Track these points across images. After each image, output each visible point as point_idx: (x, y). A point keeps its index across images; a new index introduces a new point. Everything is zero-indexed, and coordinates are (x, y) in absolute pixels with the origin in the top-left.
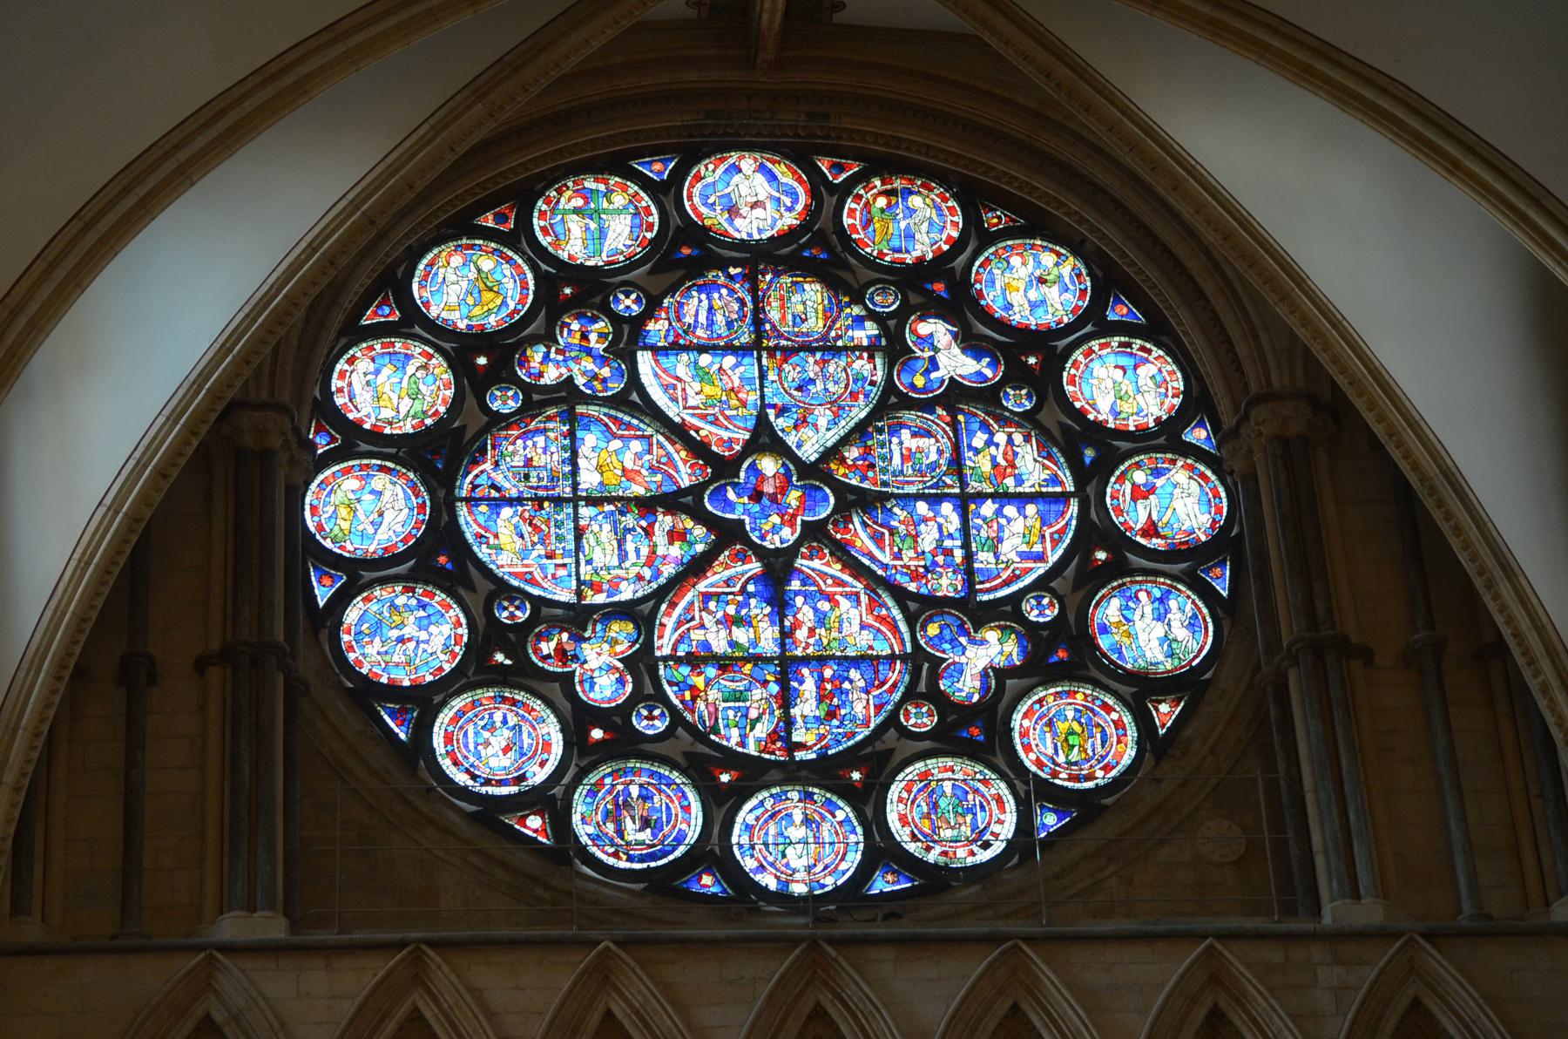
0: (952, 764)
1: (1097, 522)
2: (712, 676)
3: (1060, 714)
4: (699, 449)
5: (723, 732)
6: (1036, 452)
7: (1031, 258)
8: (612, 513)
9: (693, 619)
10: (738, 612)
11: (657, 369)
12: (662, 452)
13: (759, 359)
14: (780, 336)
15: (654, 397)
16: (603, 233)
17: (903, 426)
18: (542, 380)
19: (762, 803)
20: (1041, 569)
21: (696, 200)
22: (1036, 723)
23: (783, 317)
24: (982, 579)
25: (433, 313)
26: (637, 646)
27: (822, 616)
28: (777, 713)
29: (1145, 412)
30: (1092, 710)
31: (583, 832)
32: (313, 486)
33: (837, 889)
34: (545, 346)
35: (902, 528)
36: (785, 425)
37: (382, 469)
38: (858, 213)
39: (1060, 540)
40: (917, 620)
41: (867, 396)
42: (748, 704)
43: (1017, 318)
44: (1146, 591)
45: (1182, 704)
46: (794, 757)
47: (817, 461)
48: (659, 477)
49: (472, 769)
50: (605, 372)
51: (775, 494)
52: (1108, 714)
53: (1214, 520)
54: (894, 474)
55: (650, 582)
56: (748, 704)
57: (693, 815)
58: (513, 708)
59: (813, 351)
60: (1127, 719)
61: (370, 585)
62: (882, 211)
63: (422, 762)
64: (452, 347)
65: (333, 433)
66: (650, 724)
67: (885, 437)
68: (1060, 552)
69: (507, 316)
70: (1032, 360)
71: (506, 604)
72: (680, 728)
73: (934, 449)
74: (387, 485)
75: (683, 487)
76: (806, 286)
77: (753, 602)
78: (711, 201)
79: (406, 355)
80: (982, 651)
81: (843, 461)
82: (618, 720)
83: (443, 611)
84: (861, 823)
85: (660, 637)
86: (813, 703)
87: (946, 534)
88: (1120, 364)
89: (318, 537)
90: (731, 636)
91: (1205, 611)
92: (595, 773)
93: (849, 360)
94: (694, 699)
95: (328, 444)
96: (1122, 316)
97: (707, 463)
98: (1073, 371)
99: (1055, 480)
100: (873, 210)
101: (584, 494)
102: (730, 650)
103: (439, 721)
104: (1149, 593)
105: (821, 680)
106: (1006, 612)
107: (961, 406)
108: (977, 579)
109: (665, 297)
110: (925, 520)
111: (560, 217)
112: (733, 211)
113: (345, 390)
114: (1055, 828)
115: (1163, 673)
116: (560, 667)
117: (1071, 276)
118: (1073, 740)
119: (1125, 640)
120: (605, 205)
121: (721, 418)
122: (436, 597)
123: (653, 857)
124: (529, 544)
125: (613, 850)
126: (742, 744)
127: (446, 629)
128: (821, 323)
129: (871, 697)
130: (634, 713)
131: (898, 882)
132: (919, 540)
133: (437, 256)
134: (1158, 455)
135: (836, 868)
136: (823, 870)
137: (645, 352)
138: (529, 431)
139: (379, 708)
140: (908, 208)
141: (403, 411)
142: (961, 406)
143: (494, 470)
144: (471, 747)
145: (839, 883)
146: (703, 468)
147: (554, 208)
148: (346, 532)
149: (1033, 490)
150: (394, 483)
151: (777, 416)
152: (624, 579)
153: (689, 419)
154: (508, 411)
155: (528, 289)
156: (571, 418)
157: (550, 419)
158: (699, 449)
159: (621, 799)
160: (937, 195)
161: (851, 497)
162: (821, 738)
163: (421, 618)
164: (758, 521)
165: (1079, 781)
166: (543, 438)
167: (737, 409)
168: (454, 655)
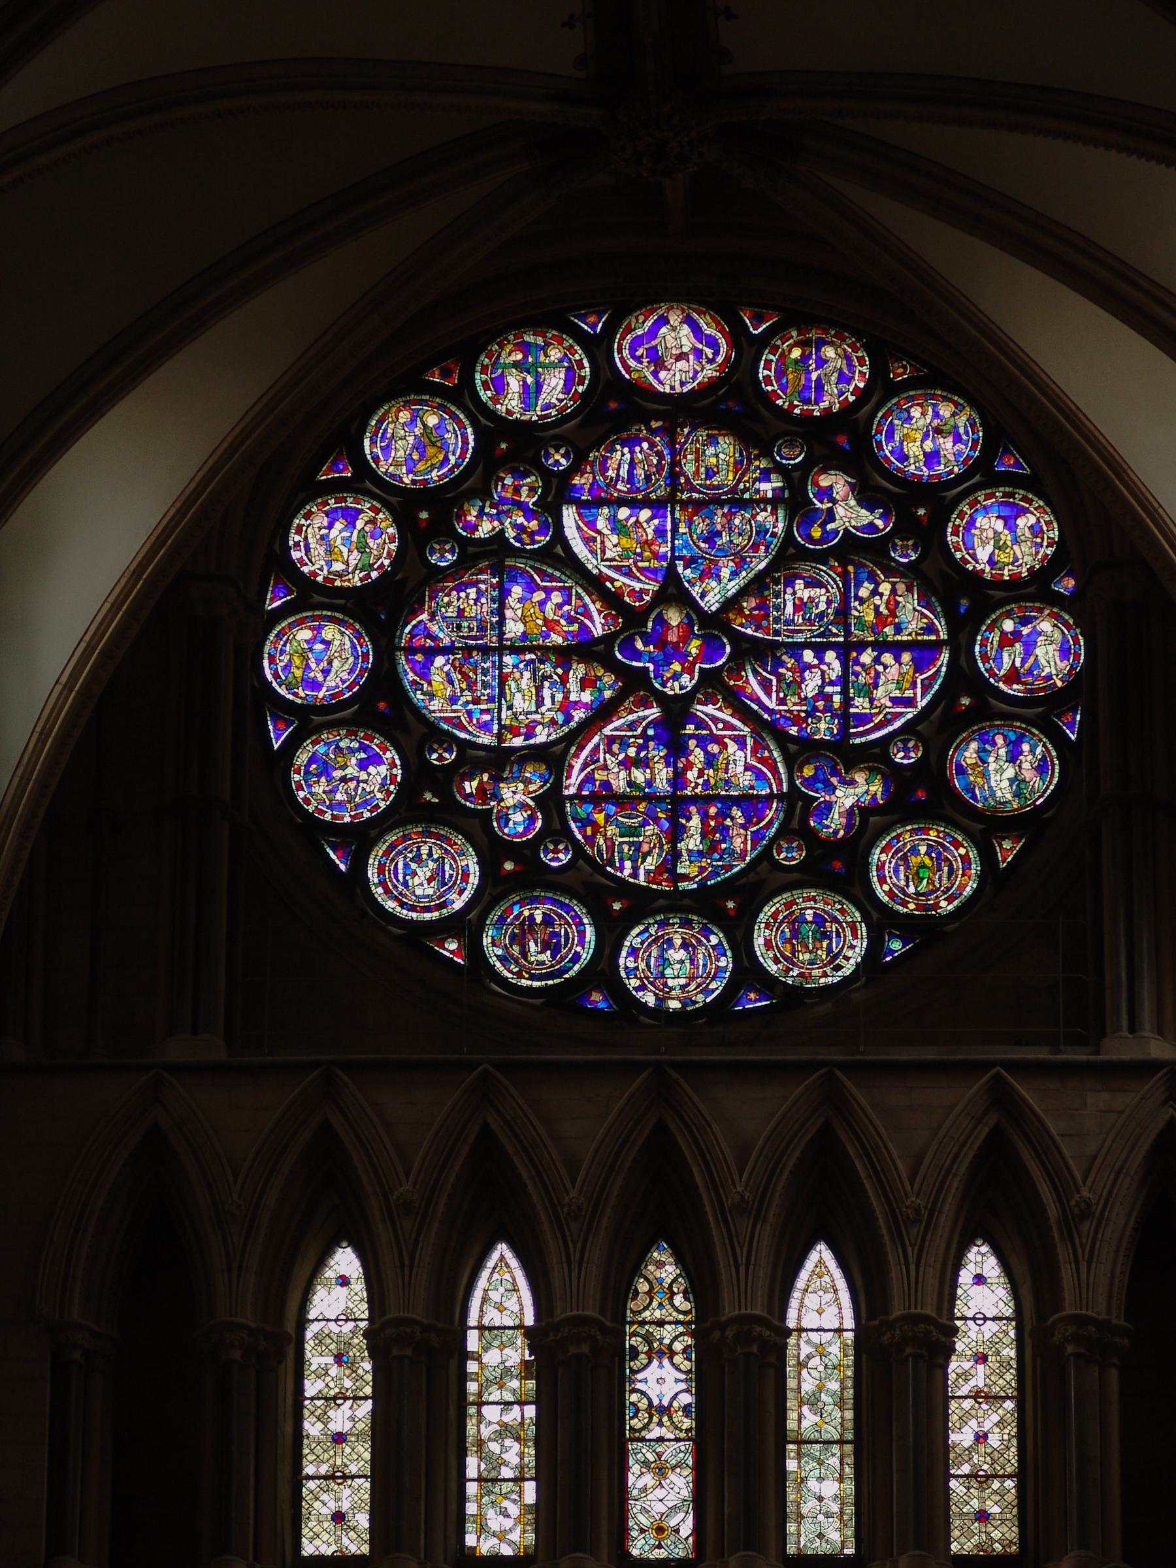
1: (966, 668)
3: (914, 851)
4: (612, 600)
5: (618, 865)
6: (916, 602)
7: (930, 409)
8: (532, 661)
9: (598, 761)
10: (638, 753)
11: (580, 522)
12: (579, 603)
14: (693, 489)
15: (576, 550)
18: (477, 533)
19: (646, 930)
23: (698, 469)
29: (1020, 561)
31: (493, 954)
32: (272, 637)
36: (691, 575)
37: (332, 620)
39: (931, 686)
42: (641, 839)
44: (1002, 734)
45: (1023, 841)
47: (718, 610)
48: (575, 627)
50: (534, 525)
51: (678, 643)
52: (957, 850)
53: (1072, 665)
55: (562, 726)
56: (641, 839)
57: (587, 940)
59: (722, 504)
61: (318, 729)
62: (796, 361)
63: (358, 891)
64: (398, 502)
67: (781, 587)
68: (929, 697)
71: (436, 746)
72: (581, 861)
73: (824, 598)
74: (336, 636)
76: (720, 439)
78: (638, 353)
82: (527, 852)
85: (569, 777)
87: (827, 680)
88: (1002, 514)
89: (274, 684)
91: (1054, 754)
93: (754, 512)
95: (285, 597)
97: (619, 614)
98: (958, 522)
99: (930, 629)
100: (788, 361)
102: (628, 790)
104: (1005, 738)
105: (705, 817)
108: (852, 723)
110: (810, 667)
111: (500, 371)
112: (658, 362)
113: (302, 544)
116: (480, 804)
117: (965, 427)
118: (924, 873)
119: (979, 780)
120: (542, 358)
121: (634, 570)
124: (458, 690)
125: (517, 969)
126: (635, 875)
128: (731, 478)
132: (803, 686)
133: (387, 412)
136: (695, 989)
141: (353, 563)
143: (431, 620)
144: (401, 880)
145: (708, 1000)
146: (615, 618)
147: (495, 362)
148: (299, 680)
149: (910, 638)
150: (342, 633)
151: (685, 568)
152: (540, 723)
153: (605, 570)
154: (445, 564)
155: (468, 444)
156: (497, 570)
157: (481, 572)
158: (612, 600)
160: (848, 345)
161: (745, 646)
162: (702, 870)
163: (361, 759)
166: (474, 590)
167: (649, 561)
168: (389, 793)
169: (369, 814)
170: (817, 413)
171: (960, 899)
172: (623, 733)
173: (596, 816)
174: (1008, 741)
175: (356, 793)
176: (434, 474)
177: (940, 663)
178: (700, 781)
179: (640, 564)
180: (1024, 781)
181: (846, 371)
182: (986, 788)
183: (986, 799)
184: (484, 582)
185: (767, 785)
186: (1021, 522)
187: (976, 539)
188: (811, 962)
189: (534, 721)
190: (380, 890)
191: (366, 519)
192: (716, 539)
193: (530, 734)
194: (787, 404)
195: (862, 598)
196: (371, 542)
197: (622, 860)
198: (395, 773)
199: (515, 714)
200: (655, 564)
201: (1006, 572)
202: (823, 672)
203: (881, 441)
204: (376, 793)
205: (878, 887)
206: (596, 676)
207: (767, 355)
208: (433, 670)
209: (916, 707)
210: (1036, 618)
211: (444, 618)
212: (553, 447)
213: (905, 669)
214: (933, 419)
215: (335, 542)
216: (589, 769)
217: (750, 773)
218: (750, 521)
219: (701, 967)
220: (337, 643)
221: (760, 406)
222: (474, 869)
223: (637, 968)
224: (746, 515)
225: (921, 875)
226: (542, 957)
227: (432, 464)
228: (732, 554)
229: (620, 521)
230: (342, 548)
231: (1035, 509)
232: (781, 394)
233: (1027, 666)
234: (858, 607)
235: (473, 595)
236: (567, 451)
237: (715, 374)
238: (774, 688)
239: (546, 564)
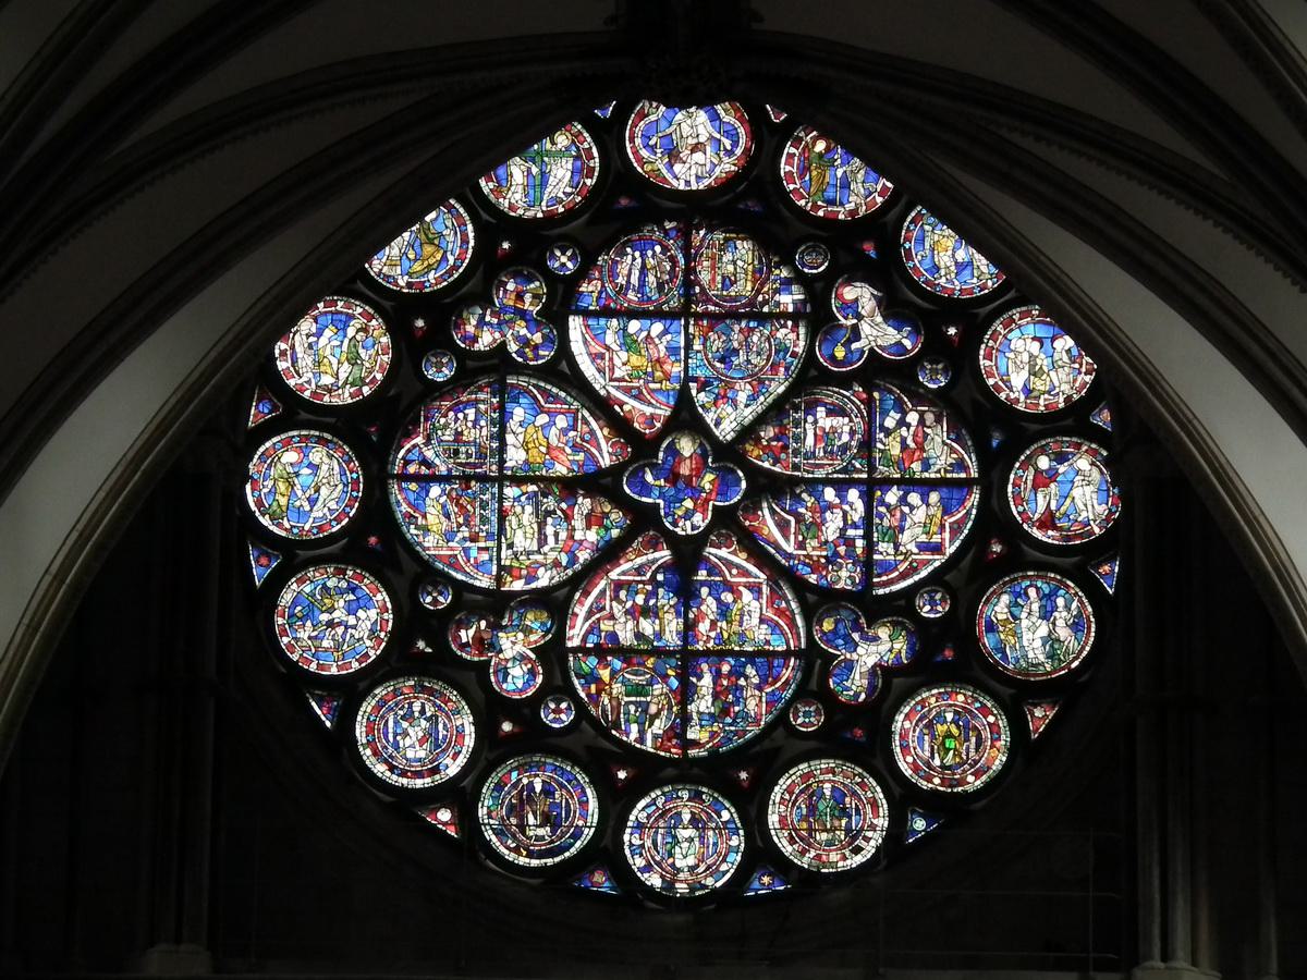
3: (940, 718)
4: (620, 426)
5: (623, 727)
6: (945, 434)
8: (535, 493)
9: (603, 608)
10: (646, 601)
12: (586, 429)
14: (708, 300)
15: (583, 367)
16: (544, 176)
17: (818, 403)
18: (476, 345)
20: (938, 561)
21: (638, 141)
22: (917, 725)
23: (714, 279)
24: (879, 571)
26: (550, 636)
27: (724, 608)
29: (1057, 390)
36: (706, 399)
37: (321, 441)
41: (787, 369)
42: (649, 699)
47: (733, 440)
48: (581, 457)
50: (537, 338)
51: (691, 476)
55: (566, 568)
56: (649, 699)
57: (590, 812)
59: (738, 317)
61: (305, 565)
62: (820, 155)
63: (345, 751)
66: (558, 716)
67: (801, 414)
68: (957, 543)
72: (584, 722)
73: (846, 429)
78: (652, 142)
79: (347, 314)
80: (873, 648)
81: (758, 440)
82: (526, 711)
85: (572, 627)
86: (709, 699)
87: (850, 522)
88: (1038, 335)
89: (257, 514)
90: (638, 628)
92: (504, 766)
97: (629, 442)
99: (960, 465)
101: (509, 473)
104: (1038, 589)
105: (717, 675)
106: (898, 609)
107: (877, 381)
110: (830, 507)
112: (673, 155)
113: (288, 353)
115: (1042, 675)
118: (950, 743)
119: (1011, 638)
120: (549, 146)
122: (365, 580)
124: (455, 525)
127: (373, 613)
128: (749, 288)
132: (824, 528)
134: (1065, 439)
136: (705, 871)
137: (577, 318)
138: (462, 402)
139: (308, 695)
141: (343, 376)
142: (877, 381)
143: (426, 444)
145: (718, 885)
148: (284, 509)
149: (938, 476)
150: (331, 457)
153: (614, 392)
155: (468, 243)
156: (501, 390)
157: (481, 389)
158: (620, 426)
162: (713, 735)
164: (672, 505)
166: (474, 410)
167: (661, 382)
169: (357, 664)
170: (841, 217)
171: (988, 774)
172: (631, 578)
174: (1041, 595)
175: (344, 640)
176: (432, 275)
178: (713, 634)
179: (652, 386)
180: (1058, 640)
183: (1017, 660)
188: (830, 843)
189: (536, 562)
190: (368, 752)
192: (733, 359)
193: (531, 578)
194: (810, 204)
195: (888, 428)
197: (627, 721)
198: (386, 618)
199: (515, 554)
200: (666, 385)
202: (845, 514)
203: (910, 248)
204: (367, 641)
205: (902, 759)
206: (603, 512)
207: (789, 149)
208: (428, 501)
209: (944, 554)
213: (932, 511)
215: (324, 352)
216: (593, 619)
217: (766, 626)
218: (768, 339)
220: (325, 467)
221: (781, 206)
222: (470, 729)
223: (642, 846)
224: (766, 331)
225: (947, 746)
226: (541, 832)
227: (429, 265)
228: (751, 376)
230: (331, 358)
233: (1063, 509)
235: (471, 417)
236: (574, 254)
237: (733, 168)
238: (793, 530)
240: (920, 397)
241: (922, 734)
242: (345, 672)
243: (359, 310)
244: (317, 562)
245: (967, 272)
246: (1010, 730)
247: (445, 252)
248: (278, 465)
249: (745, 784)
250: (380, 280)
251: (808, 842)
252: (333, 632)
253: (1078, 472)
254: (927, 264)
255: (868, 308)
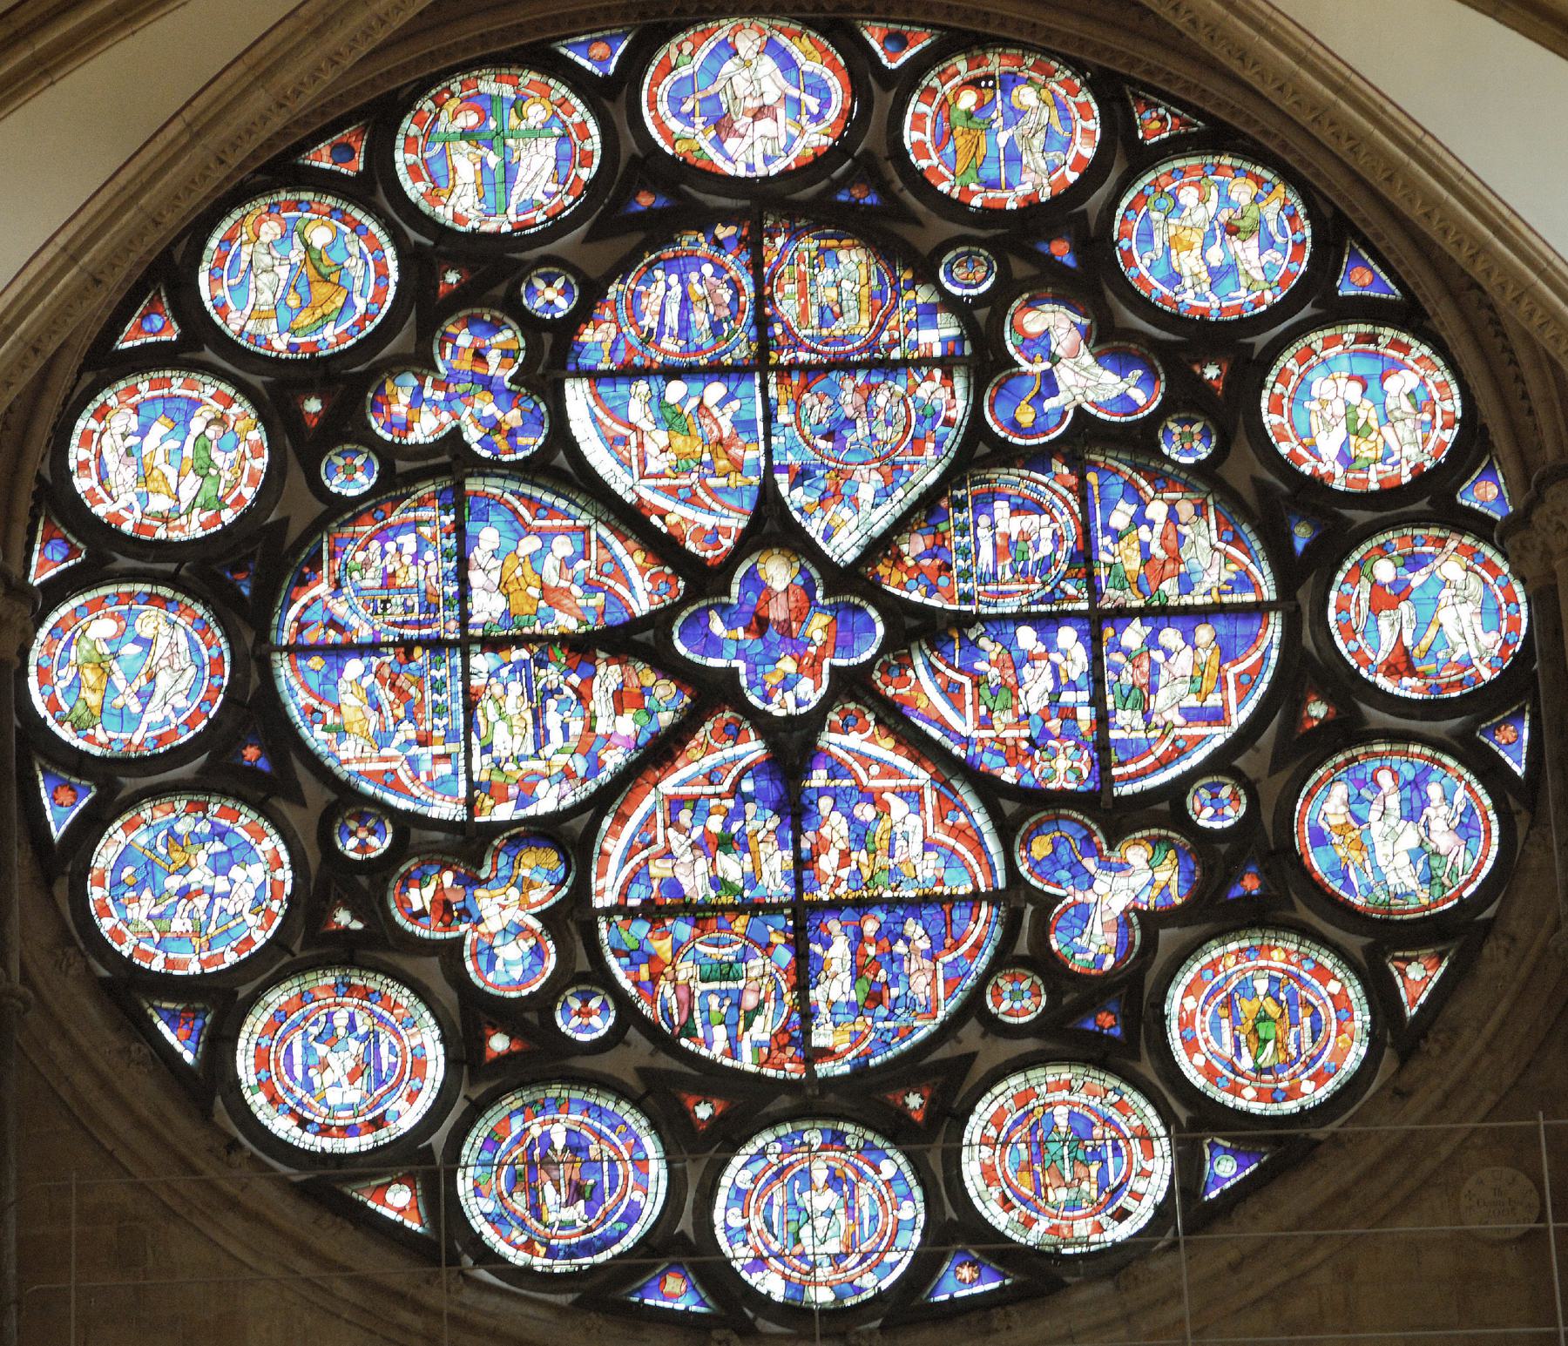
0: (1069, 1076)
1: (1314, 651)
2: (685, 939)
3: (1245, 987)
5: (700, 1033)
6: (1214, 534)
8: (525, 663)
10: (726, 826)
11: (597, 411)
12: (604, 555)
13: (764, 388)
14: (798, 345)
16: (509, 172)
17: (994, 495)
20: (1219, 736)
21: (663, 108)
22: (1206, 1002)
23: (804, 312)
24: (1122, 758)
25: (233, 326)
26: (565, 890)
28: (788, 998)
29: (1397, 456)
30: (1298, 978)
31: (477, 1209)
32: (42, 634)
33: (880, 1296)
34: (416, 375)
35: (993, 673)
36: (805, 499)
37: (151, 599)
38: (929, 121)
39: (1253, 684)
40: (1015, 830)
41: (939, 445)
43: (1189, 297)
44: (1390, 768)
45: (1445, 964)
46: (814, 1072)
47: (858, 561)
49: (299, 1110)
50: (514, 417)
51: (788, 622)
52: (1324, 983)
53: (1505, 642)
54: (982, 580)
55: (584, 780)
56: (741, 984)
57: (652, 1176)
58: (365, 1003)
59: (850, 368)
60: (1355, 991)
61: (134, 801)
62: (969, 115)
63: (218, 1099)
65: (74, 541)
67: (966, 515)
68: (1251, 706)
69: (354, 325)
70: (1211, 372)
71: (353, 825)
73: (1047, 534)
74: (161, 628)
75: (638, 614)
76: (842, 255)
77: (750, 808)
78: (687, 108)
80: (1120, 881)
81: (899, 557)
82: (532, 1017)
83: (253, 842)
84: (921, 1183)
85: (601, 874)
86: (846, 978)
87: (1064, 681)
88: (1358, 372)
89: (51, 722)
91: (1487, 801)
92: (496, 1108)
94: (654, 979)
95: (65, 560)
96: (1364, 287)
97: (678, 572)
99: (1244, 581)
100: (954, 115)
101: (479, 632)
102: (712, 894)
103: (246, 1029)
104: (1395, 774)
107: (1093, 457)
108: (1114, 759)
109: (610, 283)
110: (1030, 658)
111: (438, 147)
112: (722, 125)
113: (92, 464)
114: (1233, 1181)
115: (1415, 911)
118: (1264, 1030)
119: (1354, 854)
120: (514, 121)
121: (700, 492)
122: (242, 818)
123: (588, 1248)
124: (391, 721)
125: (524, 1238)
127: (257, 872)
128: (865, 321)
129: (939, 966)
130: (559, 1006)
131: (979, 1280)
132: (1021, 693)
133: (239, 223)
134: (1417, 532)
135: (880, 1259)
136: (860, 1263)
138: (390, 526)
139: (150, 1011)
140: (1012, 108)
142: (1093, 457)
145: (884, 1285)
147: (429, 132)
148: (96, 712)
149: (1208, 600)
150: (173, 624)
151: (793, 486)
153: (647, 495)
155: (387, 277)
157: (422, 503)
159: (537, 1151)
160: (1058, 83)
161: (911, 623)
162: (857, 1038)
163: (216, 854)
164: (760, 669)
165: (1275, 1101)
167: (726, 475)
168: (270, 916)
169: (234, 955)
170: (1011, 205)
172: (697, 790)
173: (657, 944)
175: (210, 918)
177: (1266, 643)
178: (844, 873)
179: (712, 482)
180: (1436, 854)
181: (1057, 127)
182: (1369, 869)
183: (1370, 890)
184: (428, 522)
185: (966, 876)
186: (1394, 384)
187: (1313, 419)
188: (1073, 1206)
189: (533, 773)
191: (209, 416)
192: (846, 433)
194: (957, 189)
196: (218, 457)
197: (707, 1023)
201: (1373, 476)
202: (1055, 669)
207: (916, 106)
208: (342, 686)
210: (1434, 556)
211: (358, 591)
212: (541, 276)
214: (1219, 209)
216: (637, 859)
218: (904, 399)
219: (866, 1222)
220: (162, 642)
222: (435, 1054)
223: (748, 1228)
225: (1262, 1035)
226: (568, 1214)
229: (670, 406)
230: (168, 470)
231: (1416, 361)
232: (947, 173)
233: (1424, 643)
234: (1111, 547)
238: (969, 698)
239: (540, 486)
240: (1163, 475)
241: (1217, 1017)
242: (214, 969)
243: (210, 391)
244: (156, 793)
245: (1228, 282)
246: (1369, 1002)
247: (350, 293)
248: (83, 643)
249: (918, 1117)
250: (244, 343)
251: (1035, 1202)
252: (190, 906)
253: (1444, 584)
254: (1162, 271)
255: (1065, 344)
